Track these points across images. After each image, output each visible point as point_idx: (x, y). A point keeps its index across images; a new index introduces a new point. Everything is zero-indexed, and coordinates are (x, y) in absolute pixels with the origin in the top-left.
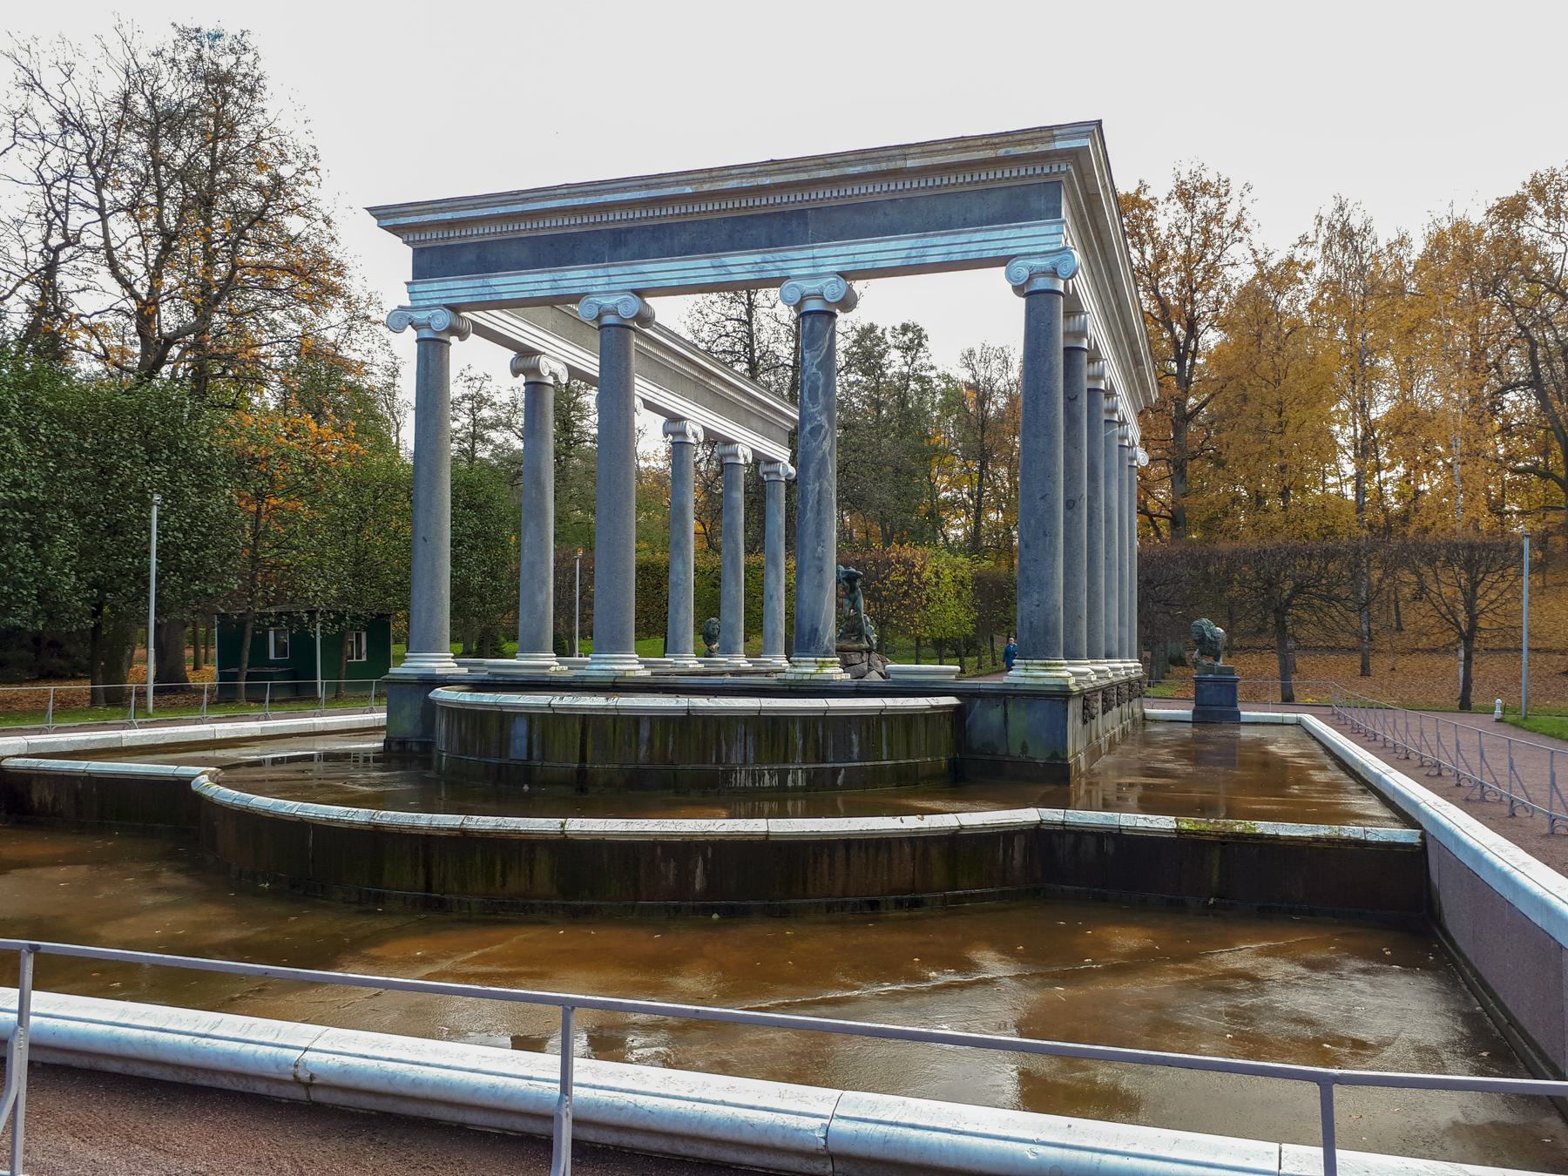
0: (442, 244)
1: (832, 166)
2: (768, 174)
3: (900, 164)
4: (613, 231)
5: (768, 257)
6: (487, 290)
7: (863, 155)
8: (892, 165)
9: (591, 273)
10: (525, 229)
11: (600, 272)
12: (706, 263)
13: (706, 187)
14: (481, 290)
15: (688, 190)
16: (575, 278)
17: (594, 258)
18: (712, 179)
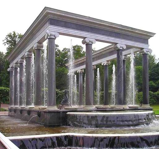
0: (57, 19)
1: (127, 28)
2: (119, 26)
3: (135, 31)
4: (91, 27)
5: (115, 39)
6: (67, 32)
7: (132, 28)
8: (134, 31)
9: (88, 34)
10: (75, 22)
11: (89, 34)
12: (107, 37)
13: (110, 25)
14: (65, 31)
15: (107, 25)
16: (84, 34)
17: (88, 31)
18: (111, 24)
